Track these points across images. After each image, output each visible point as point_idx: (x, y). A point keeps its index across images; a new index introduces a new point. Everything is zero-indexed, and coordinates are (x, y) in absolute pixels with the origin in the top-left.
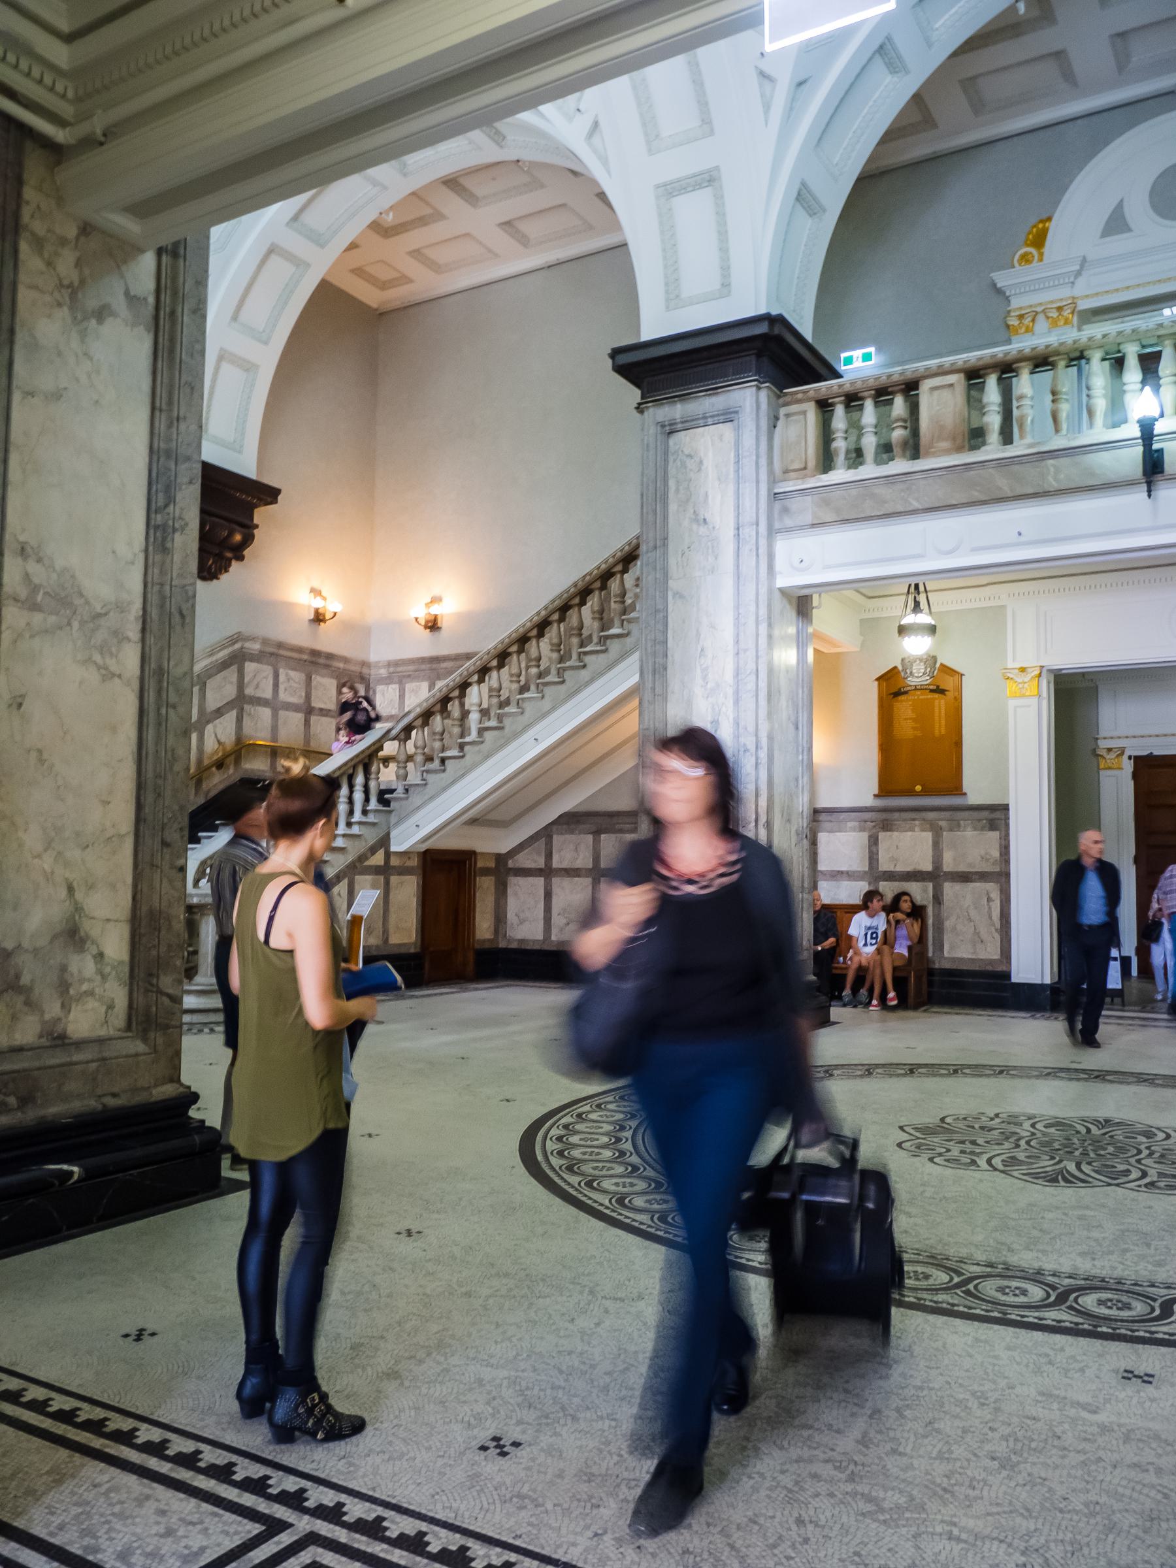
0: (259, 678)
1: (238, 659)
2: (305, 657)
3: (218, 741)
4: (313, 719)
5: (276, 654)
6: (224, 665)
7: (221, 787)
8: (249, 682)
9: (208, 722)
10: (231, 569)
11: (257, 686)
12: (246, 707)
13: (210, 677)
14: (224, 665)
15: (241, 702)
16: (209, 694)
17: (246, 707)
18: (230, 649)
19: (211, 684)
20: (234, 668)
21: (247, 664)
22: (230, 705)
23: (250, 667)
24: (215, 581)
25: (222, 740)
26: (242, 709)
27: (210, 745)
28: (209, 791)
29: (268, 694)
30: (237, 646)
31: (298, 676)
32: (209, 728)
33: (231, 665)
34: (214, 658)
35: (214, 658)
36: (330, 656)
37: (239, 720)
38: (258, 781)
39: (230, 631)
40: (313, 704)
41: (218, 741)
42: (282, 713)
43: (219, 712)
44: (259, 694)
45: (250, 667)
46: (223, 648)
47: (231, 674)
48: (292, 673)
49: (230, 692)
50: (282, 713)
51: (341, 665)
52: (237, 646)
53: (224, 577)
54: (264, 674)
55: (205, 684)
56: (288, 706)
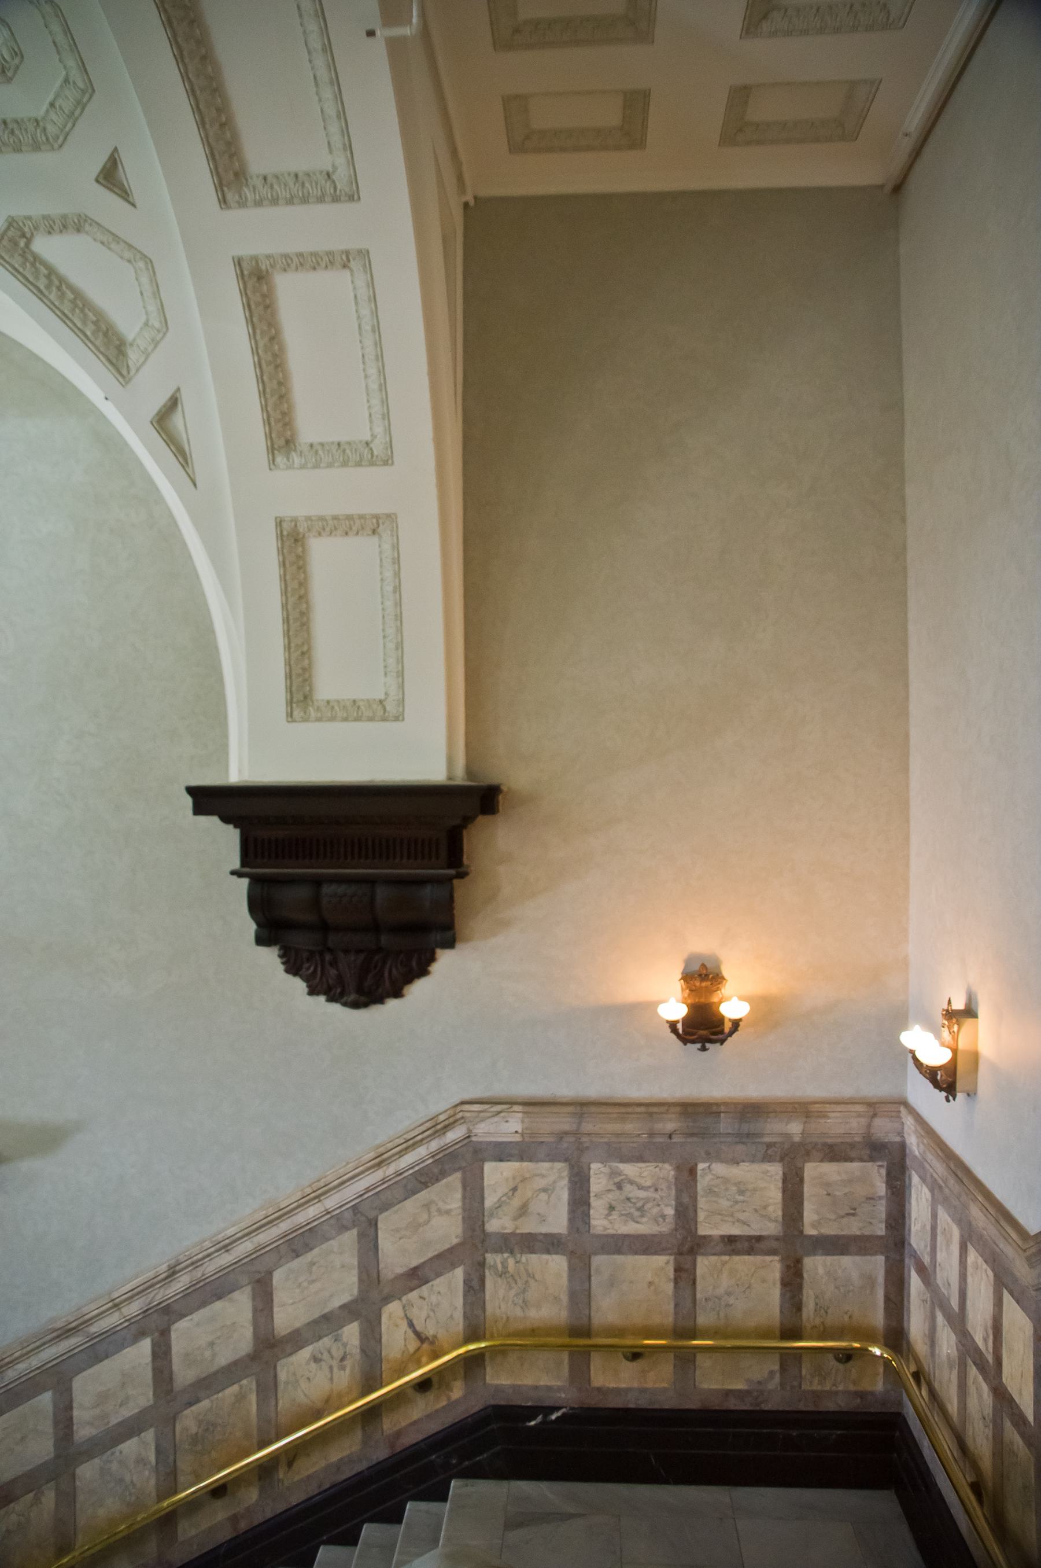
0: (528, 1195)
1: (466, 1161)
2: (670, 1126)
3: (418, 1334)
4: (704, 1264)
5: (575, 1133)
6: (424, 1178)
7: (433, 1427)
8: (500, 1204)
9: (387, 1300)
10: (435, 968)
11: (523, 1211)
12: (493, 1259)
13: (385, 1207)
14: (424, 1178)
15: (476, 1248)
16: (386, 1243)
17: (493, 1259)
18: (434, 1145)
19: (387, 1223)
20: (455, 1179)
21: (489, 1167)
22: (444, 1260)
23: (497, 1175)
24: (392, 1004)
25: (430, 1331)
26: (482, 1264)
27: (395, 1338)
28: (398, 1434)
29: (558, 1222)
30: (453, 1135)
31: (651, 1177)
32: (392, 1311)
33: (443, 1174)
34: (391, 1170)
35: (391, 1170)
36: (752, 1111)
37: (474, 1289)
38: (533, 1411)
39: (439, 1105)
40: (703, 1230)
41: (418, 1334)
42: (598, 1261)
43: (416, 1277)
44: (529, 1226)
45: (497, 1175)
46: (411, 1145)
47: (449, 1194)
48: (629, 1169)
49: (446, 1228)
50: (598, 1261)
51: (795, 1128)
52: (453, 1135)
53: (418, 990)
54: (542, 1183)
55: (374, 1223)
56: (619, 1244)
